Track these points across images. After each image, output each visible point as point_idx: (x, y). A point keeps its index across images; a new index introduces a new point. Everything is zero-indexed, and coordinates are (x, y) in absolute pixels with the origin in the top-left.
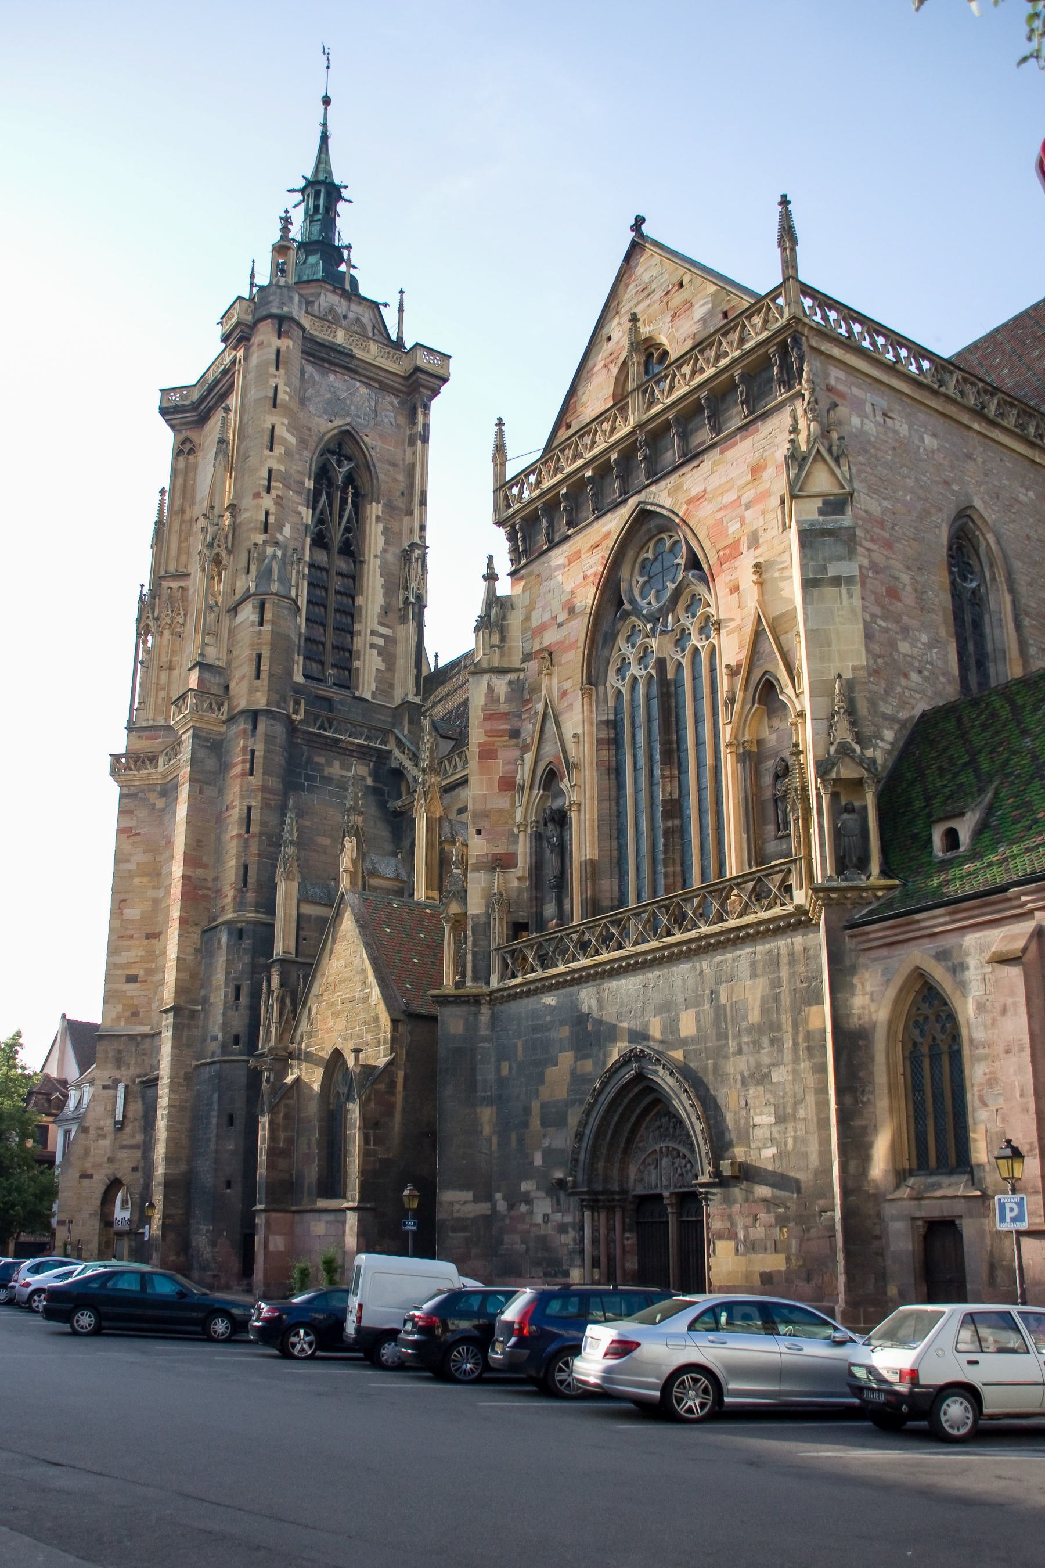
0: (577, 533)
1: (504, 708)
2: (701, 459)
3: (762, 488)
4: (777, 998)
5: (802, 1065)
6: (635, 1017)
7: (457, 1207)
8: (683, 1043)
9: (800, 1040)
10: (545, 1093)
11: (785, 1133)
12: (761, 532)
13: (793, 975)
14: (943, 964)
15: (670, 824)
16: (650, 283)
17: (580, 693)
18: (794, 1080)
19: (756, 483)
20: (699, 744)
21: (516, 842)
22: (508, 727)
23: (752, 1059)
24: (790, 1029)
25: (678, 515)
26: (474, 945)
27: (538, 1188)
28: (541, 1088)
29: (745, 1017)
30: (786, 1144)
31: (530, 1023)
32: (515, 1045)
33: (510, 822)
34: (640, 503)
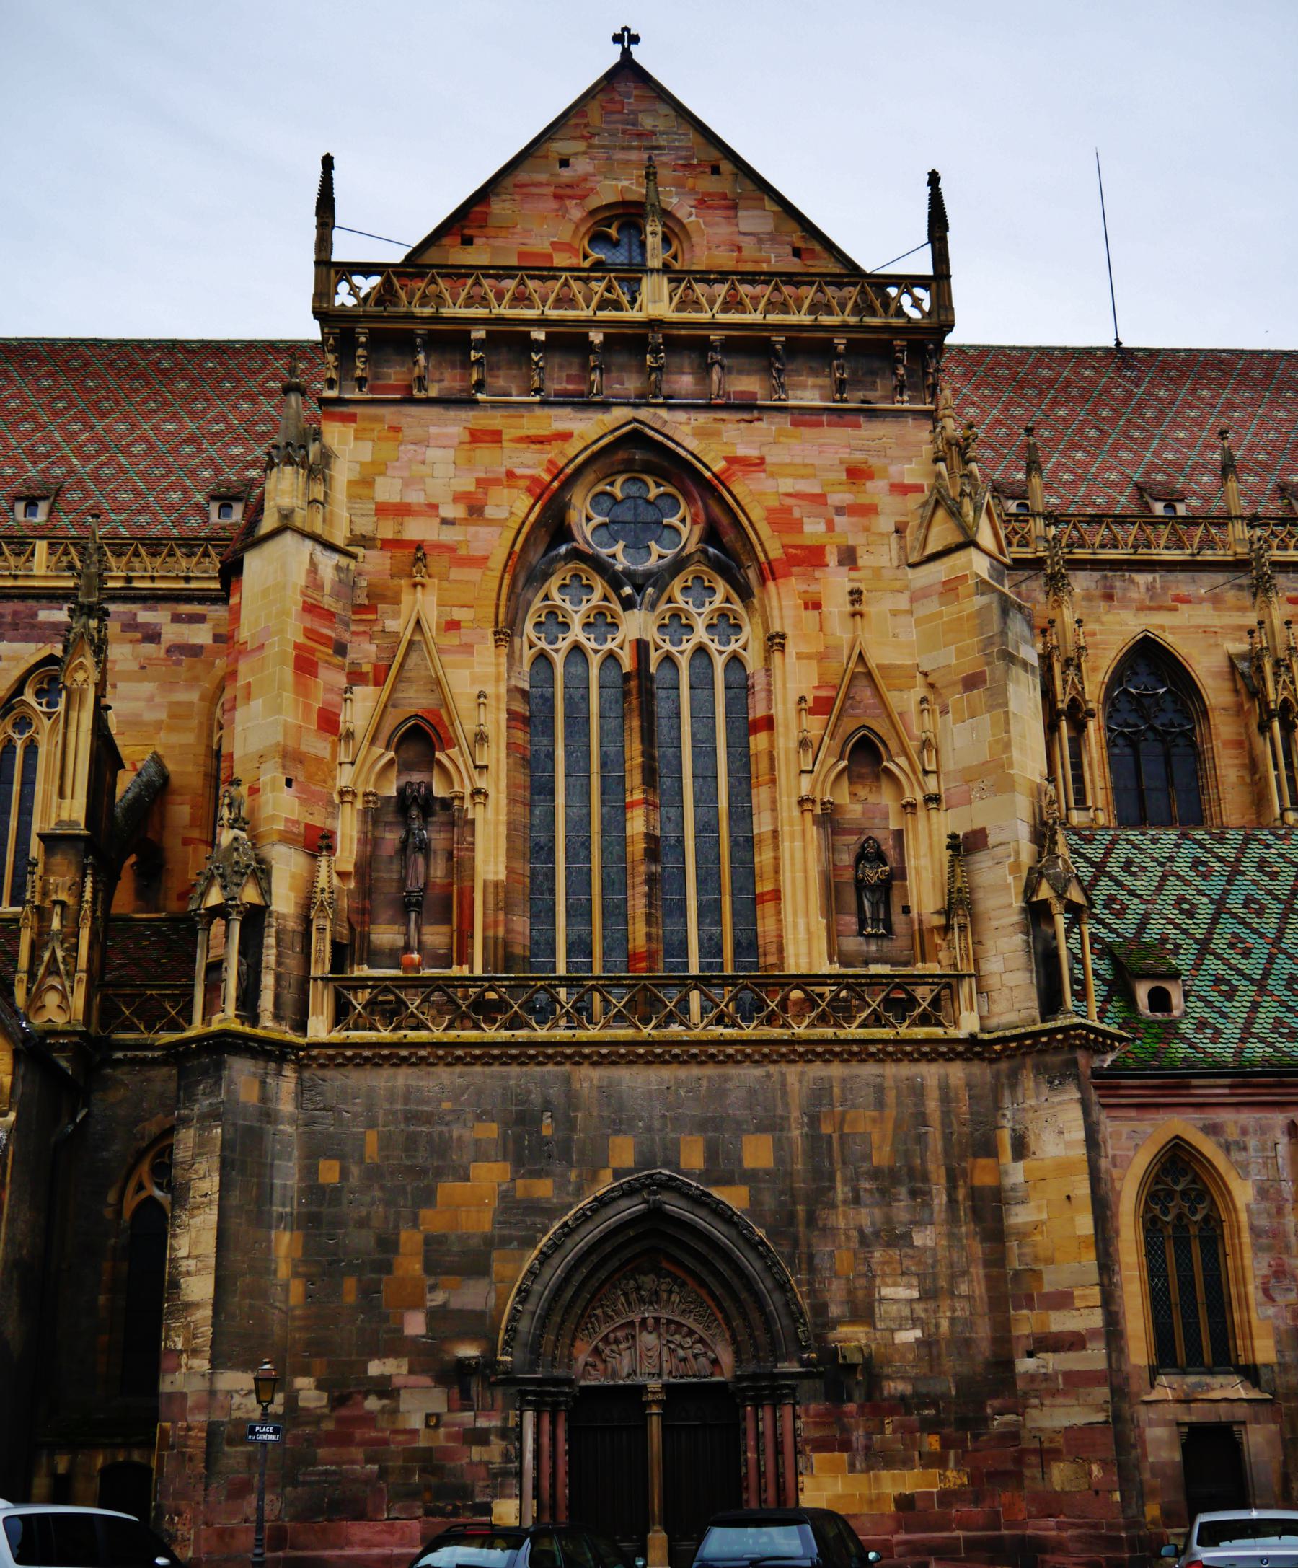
0: (494, 405)
1: (328, 602)
2: (756, 414)
3: (863, 499)
4: (921, 1139)
5: (963, 1229)
6: (649, 1129)
7: (237, 1399)
8: (751, 1178)
9: (960, 1197)
10: (432, 1220)
11: (935, 1312)
12: (860, 552)
13: (946, 1114)
14: (1214, 1139)
15: (653, 868)
16: (654, 133)
17: (491, 638)
18: (950, 1247)
19: (854, 487)
20: (706, 777)
21: (334, 816)
22: (333, 635)
23: (877, 1211)
24: (943, 1181)
25: (708, 468)
26: (279, 963)
27: (411, 1372)
28: (425, 1213)
29: (868, 1157)
30: (937, 1326)
31: (399, 1107)
32: (360, 1141)
33: (330, 783)
34: (635, 420)
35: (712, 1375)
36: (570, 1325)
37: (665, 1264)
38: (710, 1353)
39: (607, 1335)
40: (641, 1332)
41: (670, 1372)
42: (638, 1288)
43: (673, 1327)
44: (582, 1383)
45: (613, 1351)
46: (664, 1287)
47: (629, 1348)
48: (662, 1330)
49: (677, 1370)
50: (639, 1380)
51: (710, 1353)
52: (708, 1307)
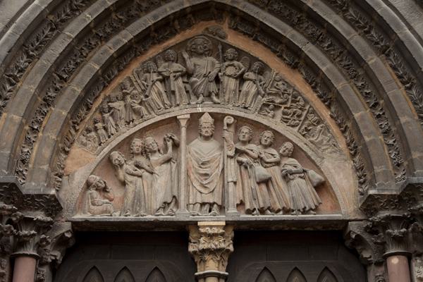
35: (316, 209)
36: (61, 110)
37: (235, 40)
38: (311, 172)
39: (129, 140)
40: (188, 141)
41: (242, 204)
42: (188, 74)
43: (245, 129)
44: (79, 217)
45: (138, 166)
46: (230, 71)
47: (168, 161)
48: (228, 134)
49: (255, 198)
50: (182, 215)
51: (311, 172)
52: (306, 102)
